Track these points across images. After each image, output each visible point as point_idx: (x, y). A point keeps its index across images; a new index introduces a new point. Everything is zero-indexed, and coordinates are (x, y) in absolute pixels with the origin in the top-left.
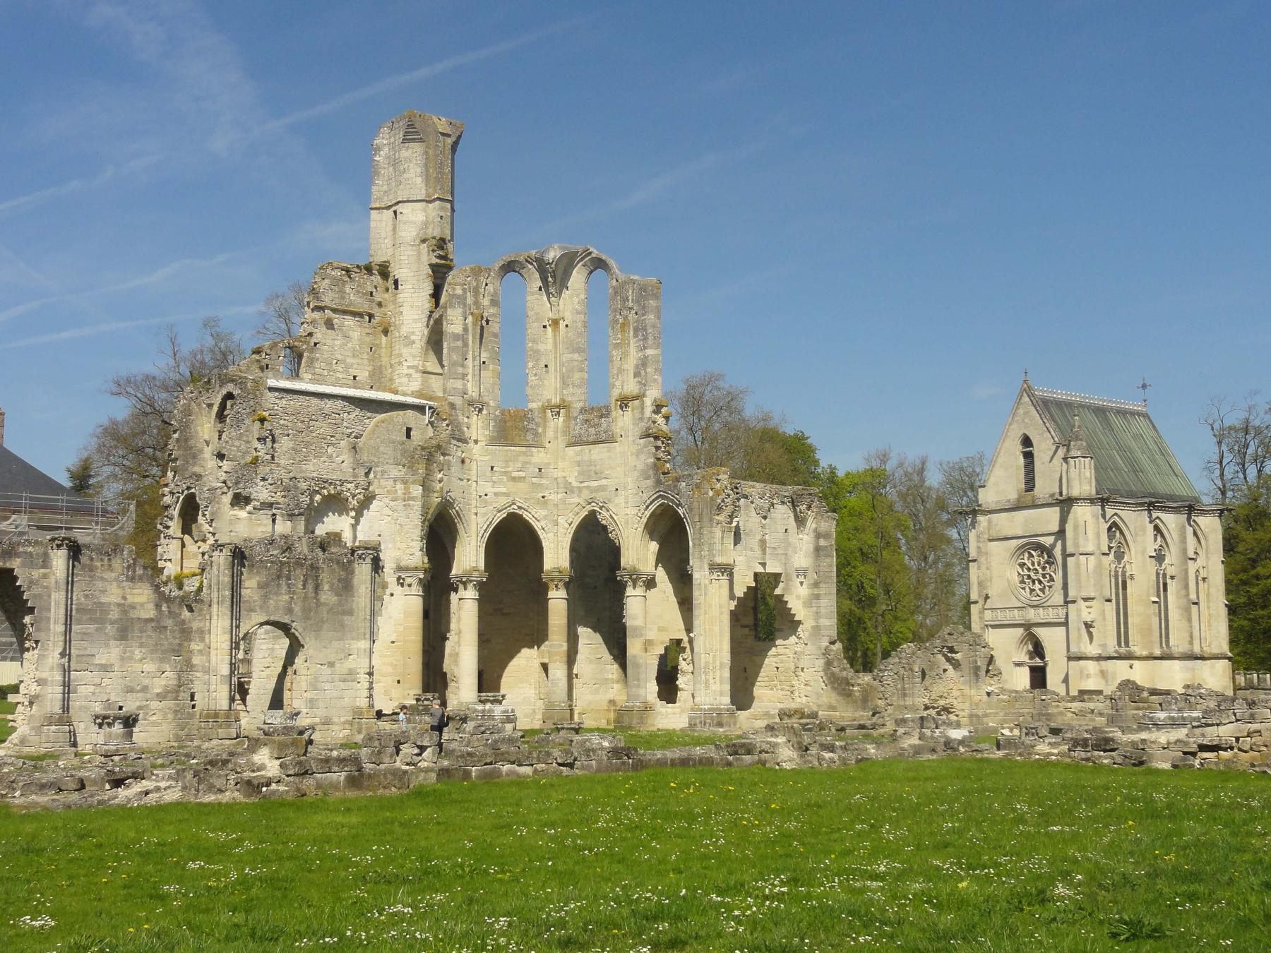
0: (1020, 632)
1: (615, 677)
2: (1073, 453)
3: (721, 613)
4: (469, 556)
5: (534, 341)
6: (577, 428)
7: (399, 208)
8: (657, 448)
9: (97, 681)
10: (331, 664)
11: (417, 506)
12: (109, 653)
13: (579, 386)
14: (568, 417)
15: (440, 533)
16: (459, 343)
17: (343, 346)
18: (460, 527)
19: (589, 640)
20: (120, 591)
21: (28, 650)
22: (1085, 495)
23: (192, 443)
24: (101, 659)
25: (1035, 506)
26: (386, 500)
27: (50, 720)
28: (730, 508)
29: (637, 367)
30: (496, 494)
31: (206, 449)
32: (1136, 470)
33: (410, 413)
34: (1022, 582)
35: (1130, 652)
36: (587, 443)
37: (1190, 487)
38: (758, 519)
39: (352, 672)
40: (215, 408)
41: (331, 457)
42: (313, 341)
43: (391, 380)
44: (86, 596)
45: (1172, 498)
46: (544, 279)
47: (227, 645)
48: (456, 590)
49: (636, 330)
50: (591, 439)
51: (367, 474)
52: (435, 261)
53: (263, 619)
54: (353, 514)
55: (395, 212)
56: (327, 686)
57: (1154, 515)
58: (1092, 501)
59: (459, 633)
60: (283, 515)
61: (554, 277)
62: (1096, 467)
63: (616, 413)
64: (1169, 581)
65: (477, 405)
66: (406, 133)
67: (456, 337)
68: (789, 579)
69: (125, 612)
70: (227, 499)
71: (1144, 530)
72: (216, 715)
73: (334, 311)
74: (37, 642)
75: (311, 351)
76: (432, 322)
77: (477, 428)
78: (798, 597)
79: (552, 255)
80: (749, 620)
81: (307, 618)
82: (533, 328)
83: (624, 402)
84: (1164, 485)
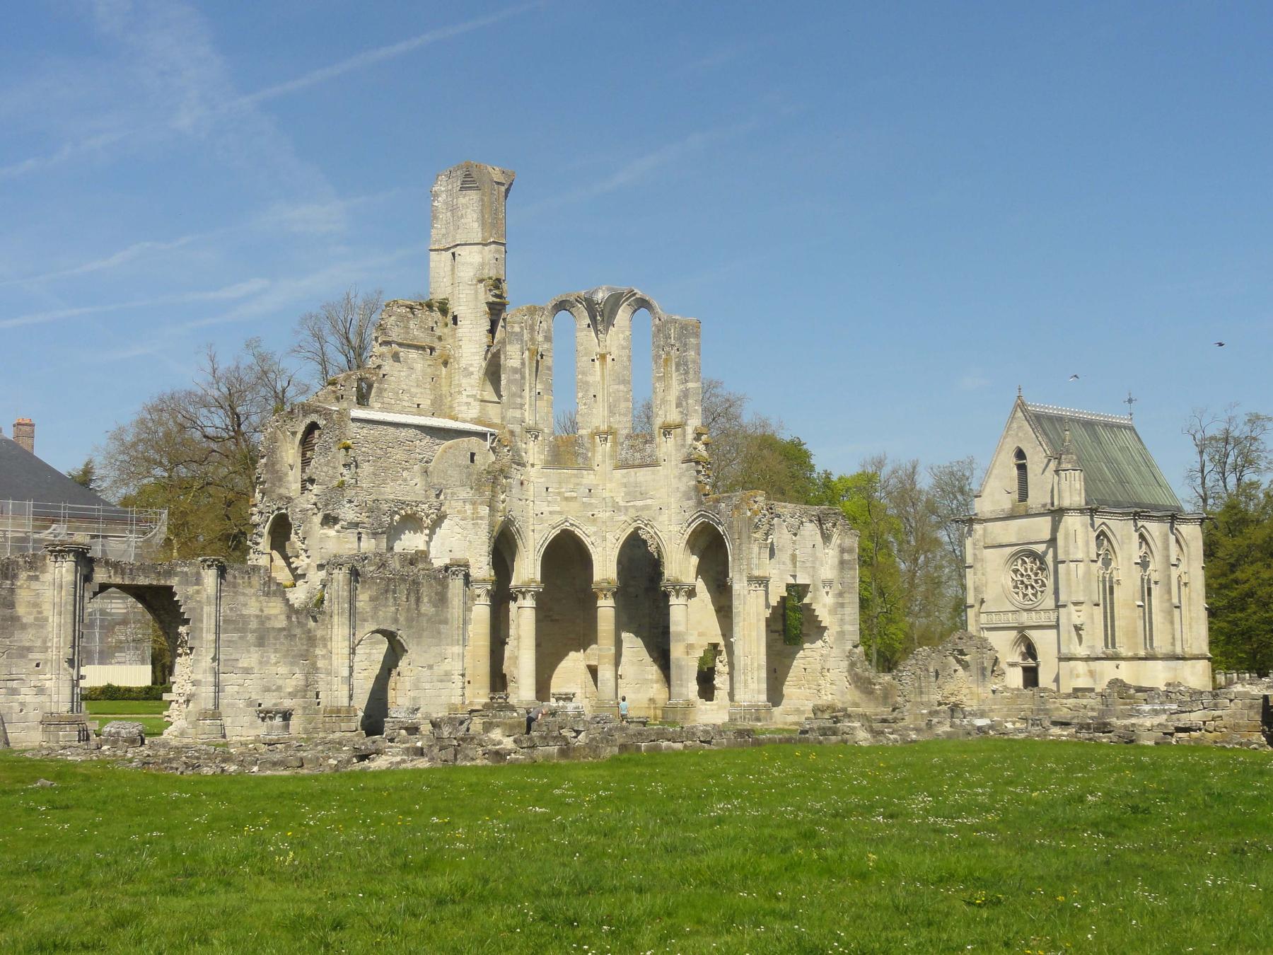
0: (1013, 634)
1: (654, 677)
2: (1064, 466)
3: (759, 620)
4: (527, 569)
5: (584, 373)
6: (624, 452)
7: (458, 250)
8: (698, 472)
9: (241, 682)
10: (430, 667)
11: (484, 524)
12: (250, 659)
13: (625, 415)
14: (615, 443)
15: (503, 548)
16: (518, 376)
17: (408, 376)
18: (519, 542)
19: (633, 645)
20: (258, 604)
21: (180, 655)
22: (1075, 506)
23: (278, 467)
24: (243, 663)
25: (1028, 515)
26: (457, 520)
27: (204, 715)
28: (766, 527)
29: (679, 398)
30: (551, 513)
31: (290, 472)
32: (1122, 481)
33: (474, 439)
34: (1016, 587)
35: (1116, 653)
36: (633, 467)
37: (1173, 496)
38: (790, 536)
39: (448, 674)
40: (299, 436)
41: (405, 480)
42: (381, 372)
43: (451, 407)
44: (231, 609)
45: (1156, 508)
46: (593, 318)
47: (346, 651)
48: (515, 600)
49: (678, 365)
50: (637, 462)
51: (438, 496)
52: (492, 299)
53: (374, 628)
54: (427, 531)
55: (453, 254)
56: (427, 686)
57: (1140, 524)
58: (1081, 511)
59: (518, 638)
60: (367, 534)
61: (601, 316)
62: (1085, 479)
63: (660, 439)
64: (1153, 586)
65: (533, 432)
66: (464, 182)
67: (515, 371)
68: (816, 589)
69: (262, 623)
70: (317, 519)
71: (1130, 538)
72: (339, 711)
73: (400, 345)
74: (191, 649)
75: (380, 382)
76: (489, 355)
77: (534, 452)
78: (824, 605)
79: (600, 296)
80: (780, 627)
81: (410, 627)
82: (584, 361)
83: (667, 430)
84: (1147, 495)
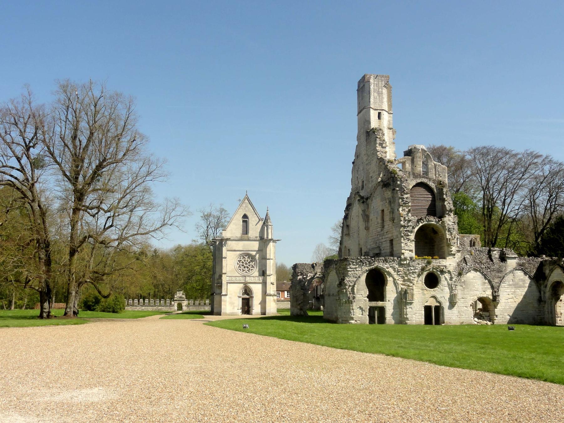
0: (242, 285)
34: (239, 267)
